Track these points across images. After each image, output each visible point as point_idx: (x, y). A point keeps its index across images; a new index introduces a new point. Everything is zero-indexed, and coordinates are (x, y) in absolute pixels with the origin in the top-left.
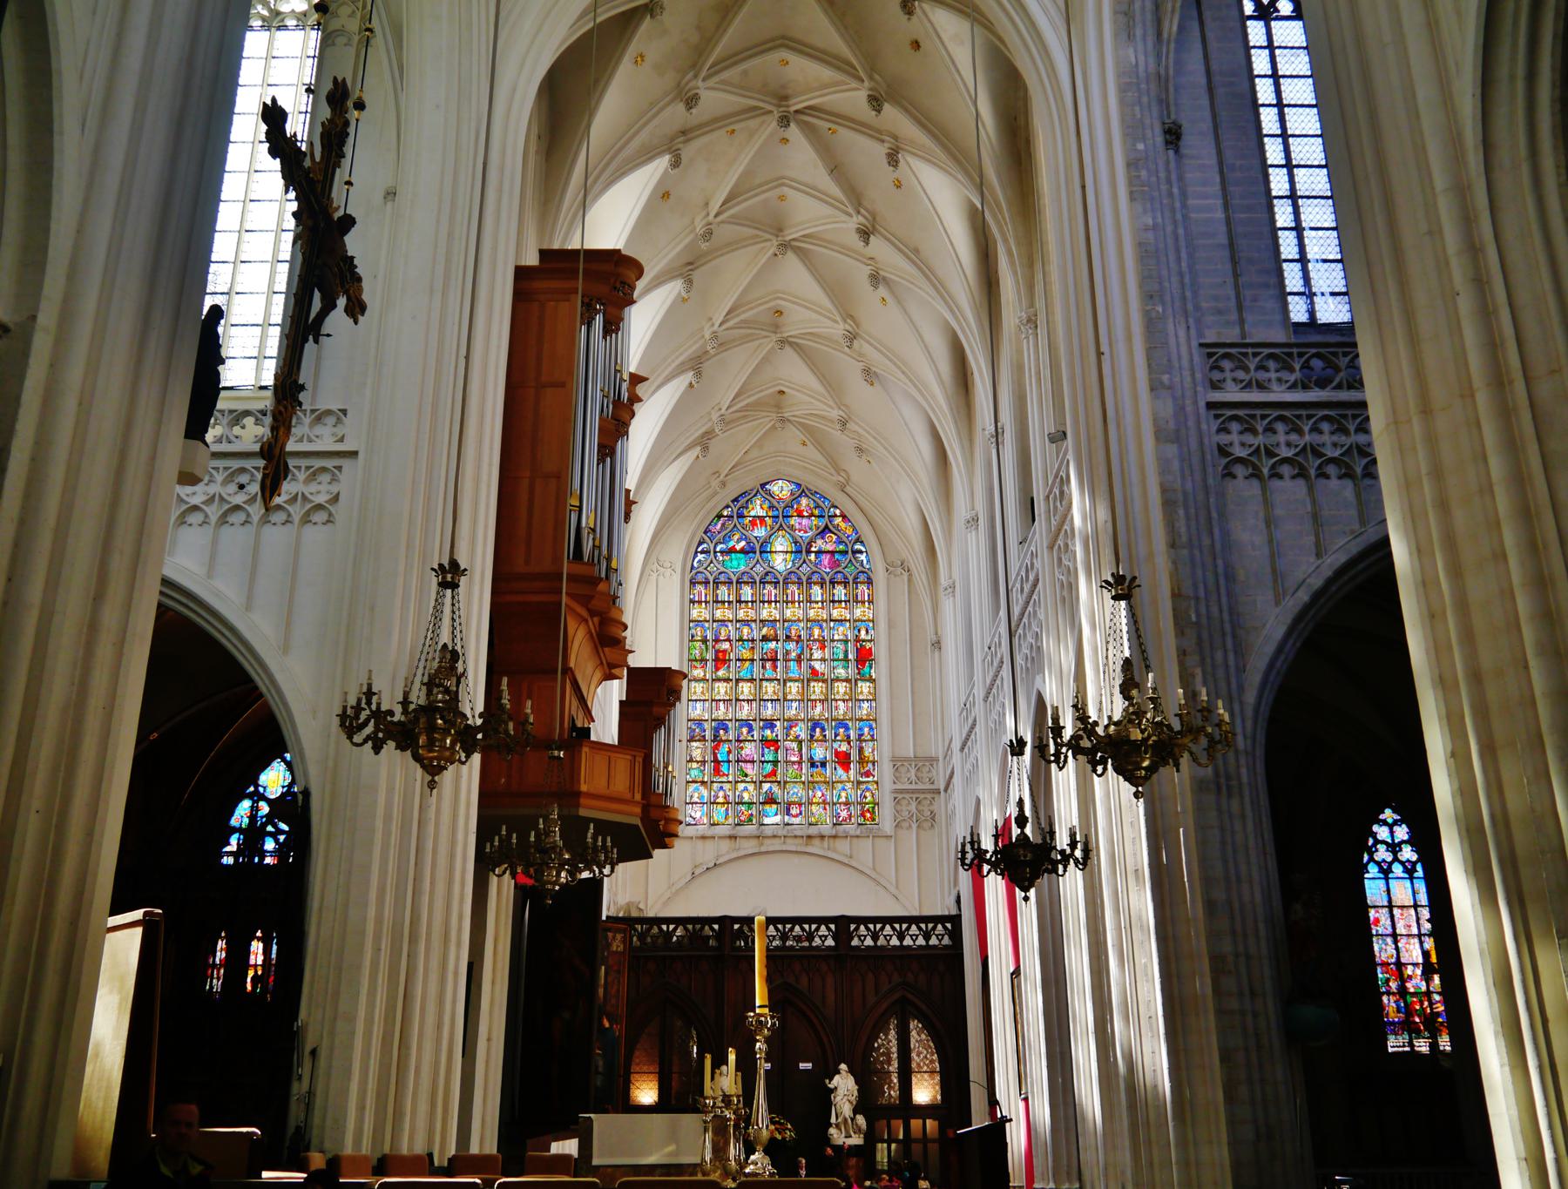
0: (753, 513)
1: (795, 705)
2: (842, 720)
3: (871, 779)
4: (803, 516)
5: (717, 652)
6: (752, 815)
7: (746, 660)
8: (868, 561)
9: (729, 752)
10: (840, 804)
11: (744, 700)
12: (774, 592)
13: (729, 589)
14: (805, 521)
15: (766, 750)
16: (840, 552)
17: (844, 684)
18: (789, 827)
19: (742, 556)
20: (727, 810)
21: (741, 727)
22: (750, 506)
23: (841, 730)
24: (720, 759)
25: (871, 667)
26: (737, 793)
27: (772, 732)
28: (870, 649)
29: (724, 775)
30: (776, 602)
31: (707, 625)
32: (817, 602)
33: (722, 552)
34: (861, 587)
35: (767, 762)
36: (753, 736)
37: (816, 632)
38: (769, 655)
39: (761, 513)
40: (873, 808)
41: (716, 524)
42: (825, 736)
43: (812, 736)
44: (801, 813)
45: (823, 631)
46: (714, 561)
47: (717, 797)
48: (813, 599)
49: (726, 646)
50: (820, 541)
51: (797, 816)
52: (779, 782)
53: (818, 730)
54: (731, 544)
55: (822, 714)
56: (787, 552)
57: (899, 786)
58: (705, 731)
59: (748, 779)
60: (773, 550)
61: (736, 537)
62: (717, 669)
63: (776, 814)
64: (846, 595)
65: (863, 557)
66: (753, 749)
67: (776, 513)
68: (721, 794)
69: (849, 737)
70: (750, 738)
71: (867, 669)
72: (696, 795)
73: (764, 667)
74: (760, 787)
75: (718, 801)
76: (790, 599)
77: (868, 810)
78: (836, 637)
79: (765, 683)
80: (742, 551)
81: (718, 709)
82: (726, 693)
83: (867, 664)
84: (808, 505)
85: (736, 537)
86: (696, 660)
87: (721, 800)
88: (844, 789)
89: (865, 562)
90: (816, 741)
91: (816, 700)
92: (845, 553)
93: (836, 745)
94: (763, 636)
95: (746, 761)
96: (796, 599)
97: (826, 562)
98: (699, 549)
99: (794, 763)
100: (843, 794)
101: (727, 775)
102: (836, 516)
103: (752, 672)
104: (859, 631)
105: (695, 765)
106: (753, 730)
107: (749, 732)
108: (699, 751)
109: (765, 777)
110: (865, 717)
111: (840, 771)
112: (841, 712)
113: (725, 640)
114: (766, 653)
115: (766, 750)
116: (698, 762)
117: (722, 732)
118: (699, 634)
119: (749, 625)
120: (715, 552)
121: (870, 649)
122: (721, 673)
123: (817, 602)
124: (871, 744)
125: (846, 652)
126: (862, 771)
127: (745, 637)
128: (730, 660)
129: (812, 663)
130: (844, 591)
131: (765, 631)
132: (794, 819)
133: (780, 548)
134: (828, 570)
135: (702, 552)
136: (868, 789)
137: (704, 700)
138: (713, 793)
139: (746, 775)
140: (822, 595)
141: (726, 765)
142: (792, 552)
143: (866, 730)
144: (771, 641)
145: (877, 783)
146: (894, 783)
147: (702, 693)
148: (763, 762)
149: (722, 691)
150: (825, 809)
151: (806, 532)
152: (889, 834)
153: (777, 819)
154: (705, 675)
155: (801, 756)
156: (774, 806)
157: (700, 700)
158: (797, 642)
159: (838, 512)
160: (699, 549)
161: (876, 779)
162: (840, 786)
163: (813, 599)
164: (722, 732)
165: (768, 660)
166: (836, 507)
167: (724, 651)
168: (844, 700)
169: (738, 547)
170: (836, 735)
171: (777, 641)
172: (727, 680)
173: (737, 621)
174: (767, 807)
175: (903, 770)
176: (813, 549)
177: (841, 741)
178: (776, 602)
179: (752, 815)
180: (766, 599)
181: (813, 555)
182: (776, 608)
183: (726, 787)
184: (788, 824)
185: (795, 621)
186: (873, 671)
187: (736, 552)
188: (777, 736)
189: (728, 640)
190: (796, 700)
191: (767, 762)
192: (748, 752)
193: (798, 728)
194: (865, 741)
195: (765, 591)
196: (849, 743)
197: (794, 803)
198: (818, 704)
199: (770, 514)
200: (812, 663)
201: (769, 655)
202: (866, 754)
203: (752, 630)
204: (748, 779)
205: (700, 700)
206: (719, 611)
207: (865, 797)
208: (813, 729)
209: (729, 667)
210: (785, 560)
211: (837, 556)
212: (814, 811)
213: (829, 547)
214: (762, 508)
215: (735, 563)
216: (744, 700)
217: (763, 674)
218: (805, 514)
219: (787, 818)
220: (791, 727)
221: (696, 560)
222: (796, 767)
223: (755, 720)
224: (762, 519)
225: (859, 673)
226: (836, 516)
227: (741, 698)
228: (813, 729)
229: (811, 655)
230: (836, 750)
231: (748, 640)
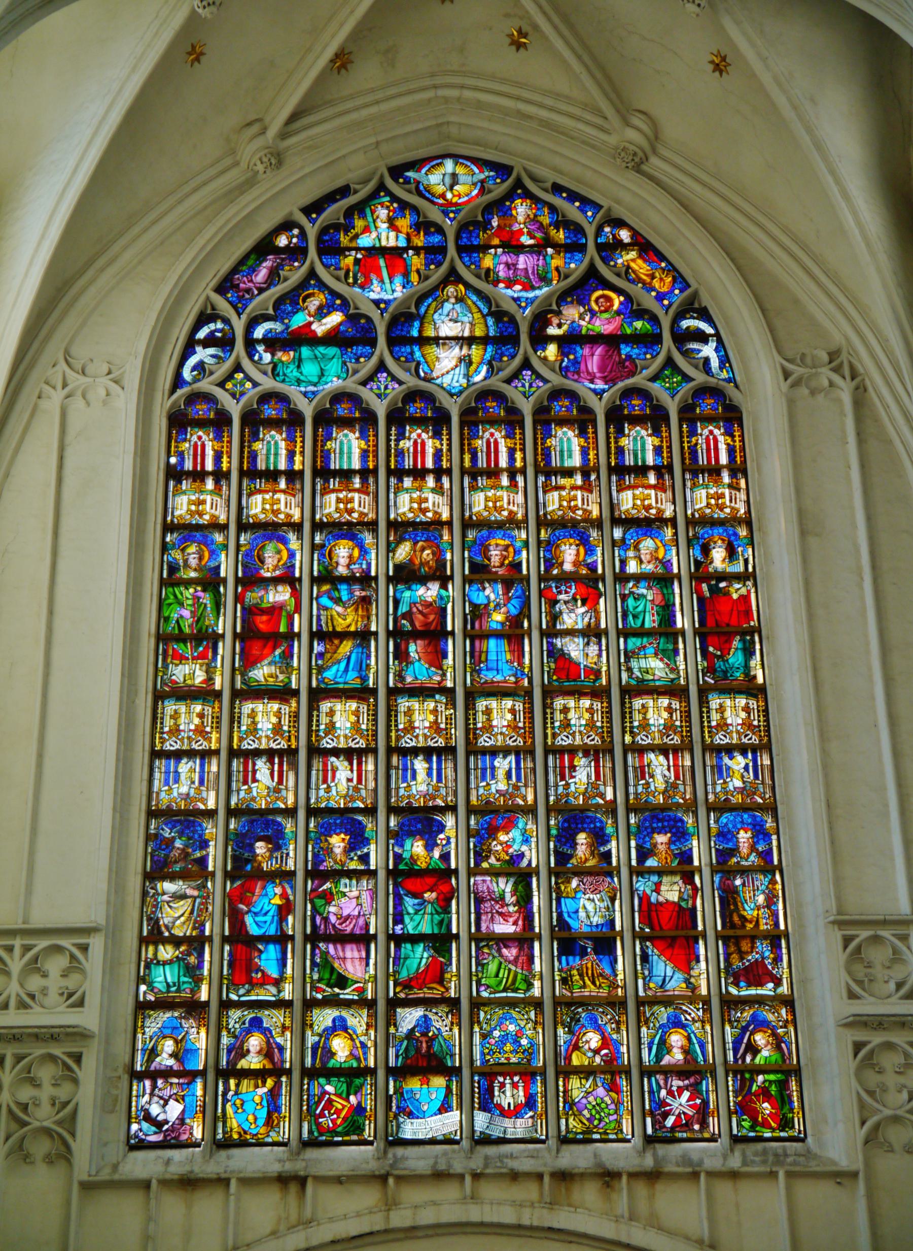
0: (365, 241)
1: (503, 764)
2: (663, 808)
3: (767, 990)
4: (520, 249)
5: (251, 612)
6: (359, 1110)
7: (343, 636)
8: (725, 361)
9: (285, 910)
10: (668, 1072)
11: (336, 752)
12: (431, 446)
13: (291, 439)
14: (523, 261)
15: (410, 903)
16: (636, 339)
17: (664, 702)
18: (491, 1150)
19: (332, 351)
20: (274, 1094)
21: (327, 831)
22: (359, 224)
23: (661, 839)
24: (254, 930)
25: (749, 652)
26: (311, 1040)
27: (430, 846)
28: (745, 599)
29: (266, 980)
30: (439, 472)
31: (218, 538)
32: (569, 473)
33: (271, 343)
34: (704, 431)
35: (415, 939)
36: (365, 859)
37: (569, 554)
38: (419, 619)
39: (390, 239)
40: (783, 1085)
41: (253, 270)
42: (607, 856)
43: (563, 858)
44: (530, 1102)
45: (590, 551)
46: (246, 363)
47: (240, 1052)
48: (555, 462)
49: (281, 595)
50: (572, 313)
51: (515, 1112)
52: (454, 1004)
53: (582, 838)
54: (299, 320)
55: (593, 789)
56: (470, 341)
57: (869, 1007)
58: (204, 844)
59: (348, 994)
60: (430, 332)
61: (313, 304)
62: (249, 661)
63: (444, 1108)
64: (658, 450)
65: (708, 351)
66: (366, 897)
67: (436, 239)
68: (255, 1042)
69: (686, 857)
70: (353, 865)
71: (736, 658)
72: (169, 1046)
73: (401, 655)
74: (391, 1020)
75: (243, 1064)
76: (482, 463)
77: (765, 1093)
78: (632, 567)
79: (404, 703)
80: (333, 338)
81: (249, 777)
82: (277, 729)
83: (736, 643)
84: (533, 220)
85: (313, 304)
86: (181, 638)
87: (253, 1062)
88: (677, 1024)
89: (715, 363)
90: (580, 873)
91: (572, 751)
92: (651, 340)
93: (643, 885)
94: (397, 567)
95: (342, 939)
96: (503, 462)
97: (593, 365)
98: (202, 334)
99: (504, 940)
100: (676, 1039)
101: (278, 982)
102: (619, 245)
103: (362, 669)
104: (706, 550)
105: (166, 952)
106: (366, 842)
107: (351, 847)
108: (183, 906)
109: (407, 985)
110: (737, 799)
111: (661, 967)
112: (659, 783)
113: (276, 581)
114: (408, 615)
115: (410, 903)
116: (176, 942)
117: (261, 848)
118: (193, 562)
119: (352, 537)
120: (250, 344)
121: (745, 599)
122: (262, 673)
123: (569, 473)
124: (762, 881)
125: (667, 611)
126: (737, 964)
127: (342, 570)
128: (291, 636)
129: (558, 642)
130: (651, 442)
131: (403, 552)
132: (508, 1123)
133: (447, 329)
134: (600, 385)
135: (208, 342)
136: (760, 1024)
137: (205, 755)
138: (225, 1040)
139: (342, 982)
140: (584, 452)
141: (272, 951)
142: (485, 340)
143: (744, 837)
144: (423, 580)
145: (789, 1002)
146: (852, 995)
147: (200, 731)
148: (399, 940)
149: (265, 725)
150: (613, 1088)
151: (528, 287)
152: (844, 1163)
153: (450, 1122)
154: (210, 679)
155: (528, 918)
156: (439, 1082)
157: (191, 754)
158: (508, 584)
159: (625, 235)
160: (202, 334)
161: (784, 989)
162: (663, 1014)
163: (555, 462)
164: (261, 848)
165: (415, 635)
166: (619, 223)
167: (276, 610)
168: (664, 750)
169: (320, 328)
170: (643, 855)
171: (444, 581)
172: (283, 694)
173: (317, 526)
174: (413, 1084)
175: (878, 955)
176: (552, 331)
177: (660, 872)
178: (439, 472)
179: (359, 1110)
180: (408, 463)
181: (552, 351)
182: (438, 490)
183: (273, 1019)
184: (486, 1140)
185: (500, 525)
186: (755, 662)
187: (314, 341)
188: (445, 857)
189: (288, 578)
190: (506, 751)
191: (415, 939)
192: (348, 907)
193: (515, 834)
194: (744, 872)
195: (406, 444)
196: (688, 878)
197: (507, 1070)
198: (580, 761)
199: (419, 241)
200: (558, 642)
201: (419, 619)
202: (749, 912)
203: (364, 551)
204: (348, 994)
205: (191, 754)
206: (259, 498)
207: (754, 1050)
208: (566, 837)
209: (288, 655)
210: (466, 361)
211: (625, 350)
212: (577, 1095)
213: (601, 326)
214: (392, 226)
215: (310, 370)
216: (336, 752)
217: (400, 676)
218: (526, 240)
219: (481, 1120)
220: (492, 831)
221: (192, 361)
222: (510, 953)
223: (371, 811)
224: (393, 254)
225: (710, 670)
226: (619, 245)
227: (327, 743)
228: (566, 837)
229: (555, 617)
230: (644, 899)
231: (349, 580)
